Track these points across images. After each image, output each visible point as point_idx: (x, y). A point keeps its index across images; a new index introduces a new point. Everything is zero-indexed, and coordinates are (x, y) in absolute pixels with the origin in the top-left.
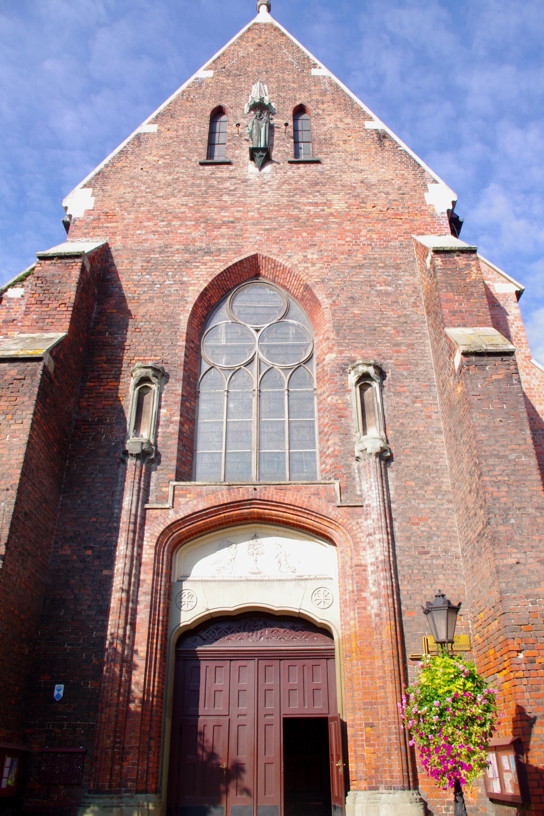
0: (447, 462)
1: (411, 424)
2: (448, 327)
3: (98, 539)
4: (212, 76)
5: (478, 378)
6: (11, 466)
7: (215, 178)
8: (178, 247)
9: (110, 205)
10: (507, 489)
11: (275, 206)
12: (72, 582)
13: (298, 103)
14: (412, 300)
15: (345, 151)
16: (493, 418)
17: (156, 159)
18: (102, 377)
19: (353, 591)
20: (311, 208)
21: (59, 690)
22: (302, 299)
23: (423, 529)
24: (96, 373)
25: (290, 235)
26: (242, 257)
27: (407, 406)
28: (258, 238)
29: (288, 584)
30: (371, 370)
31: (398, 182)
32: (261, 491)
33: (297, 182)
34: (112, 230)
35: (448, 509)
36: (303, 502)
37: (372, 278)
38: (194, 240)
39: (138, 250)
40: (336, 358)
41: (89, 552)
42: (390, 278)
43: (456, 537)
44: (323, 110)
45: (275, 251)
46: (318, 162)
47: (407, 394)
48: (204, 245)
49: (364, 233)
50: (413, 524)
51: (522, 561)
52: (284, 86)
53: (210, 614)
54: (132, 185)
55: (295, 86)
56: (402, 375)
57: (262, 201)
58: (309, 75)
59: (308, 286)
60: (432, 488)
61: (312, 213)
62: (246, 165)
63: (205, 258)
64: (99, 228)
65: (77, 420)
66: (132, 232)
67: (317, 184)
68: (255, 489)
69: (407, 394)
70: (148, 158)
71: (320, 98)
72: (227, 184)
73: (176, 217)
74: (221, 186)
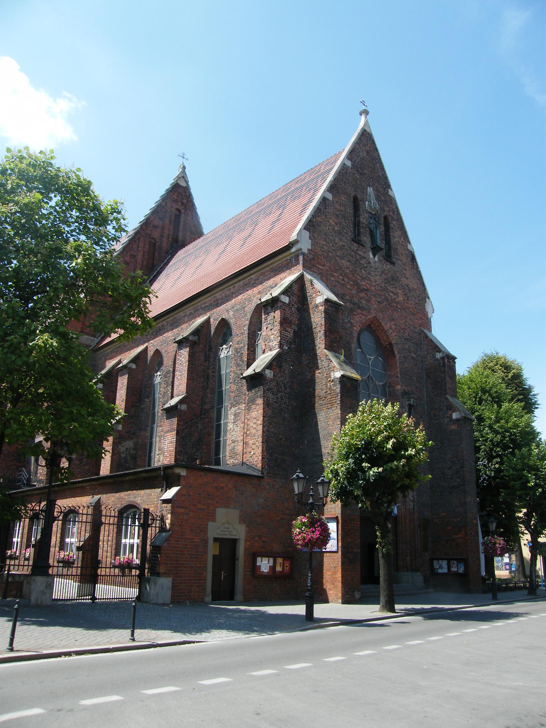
7: (359, 255)
45: (381, 317)
46: (393, 264)
58: (387, 193)
62: (369, 251)
63: (359, 310)
67: (393, 279)
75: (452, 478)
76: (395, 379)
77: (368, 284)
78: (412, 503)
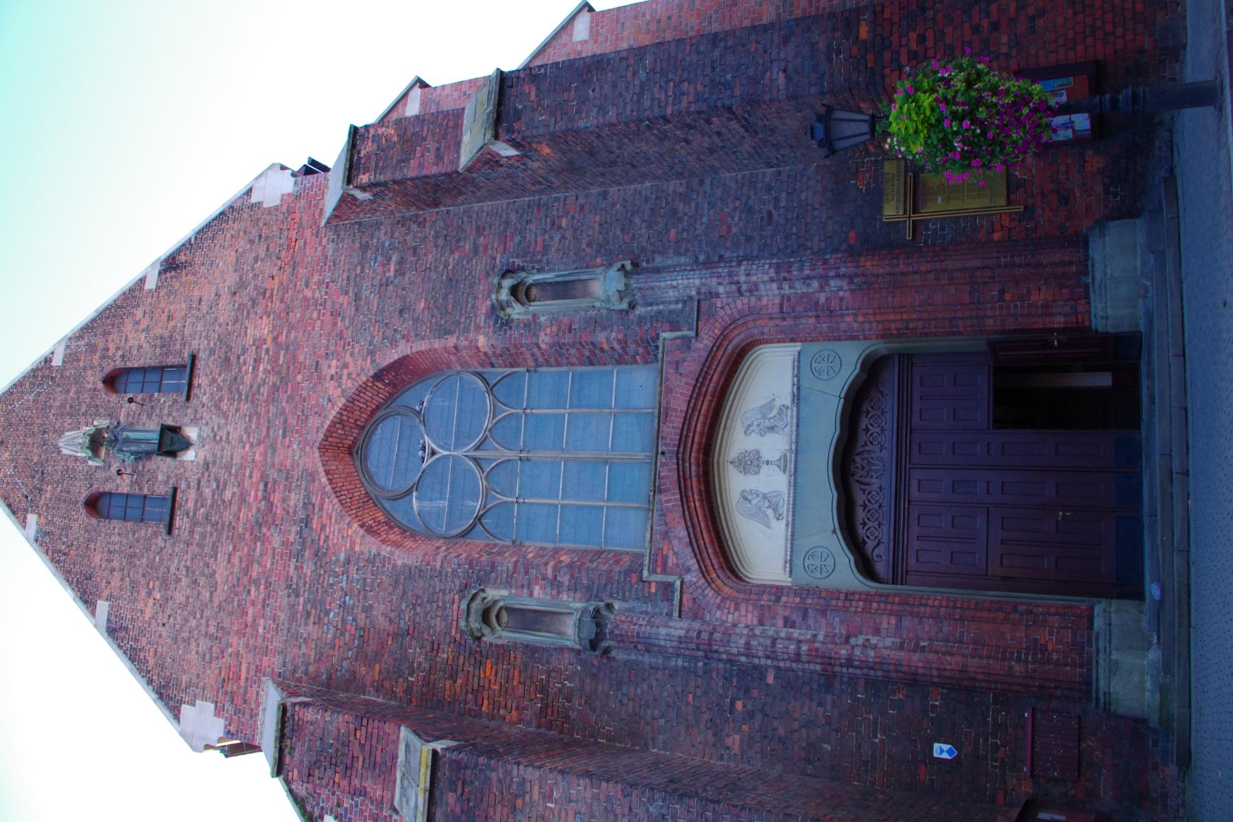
0: (647, 184)
1: (590, 232)
2: (458, 166)
3: (721, 691)
4: (35, 516)
5: (532, 120)
6: (595, 797)
8: (292, 567)
9: (211, 676)
10: (686, 84)
11: (250, 421)
12: (781, 731)
13: (100, 385)
14: (415, 227)
15: (185, 318)
16: (588, 100)
17: (151, 602)
18: (476, 687)
19: (817, 317)
20: (261, 369)
21: (942, 750)
22: (395, 386)
23: (736, 219)
24: (470, 696)
25: (297, 398)
26: (321, 470)
27: (563, 237)
28: (295, 446)
29: (803, 414)
30: (508, 283)
31: (242, 244)
32: (667, 445)
33: (220, 389)
34: (252, 673)
35: (712, 184)
36: (687, 383)
37: (376, 282)
38: (286, 544)
39: (289, 631)
40: (486, 335)
41: (739, 705)
42: (379, 258)
43: (751, 176)
44: (118, 349)
45: (318, 421)
46: (194, 358)
47: (547, 236)
48: (295, 529)
49: (308, 293)
50: (729, 231)
51: (782, 65)
52: (71, 407)
53: (841, 529)
54: (187, 641)
55: (73, 389)
56: (519, 244)
57: (241, 441)
58: (59, 369)
59: (376, 375)
60: (681, 205)
61: (269, 367)
62: (182, 462)
64: (246, 692)
65: (539, 727)
66: (260, 640)
67: (227, 359)
68: (663, 453)
69: (547, 236)
70: (147, 616)
71: (98, 354)
72: (207, 492)
73: (246, 571)
74: (209, 502)
75: (719, 134)
76: (464, 353)
77: (251, 477)
78: (832, 283)
